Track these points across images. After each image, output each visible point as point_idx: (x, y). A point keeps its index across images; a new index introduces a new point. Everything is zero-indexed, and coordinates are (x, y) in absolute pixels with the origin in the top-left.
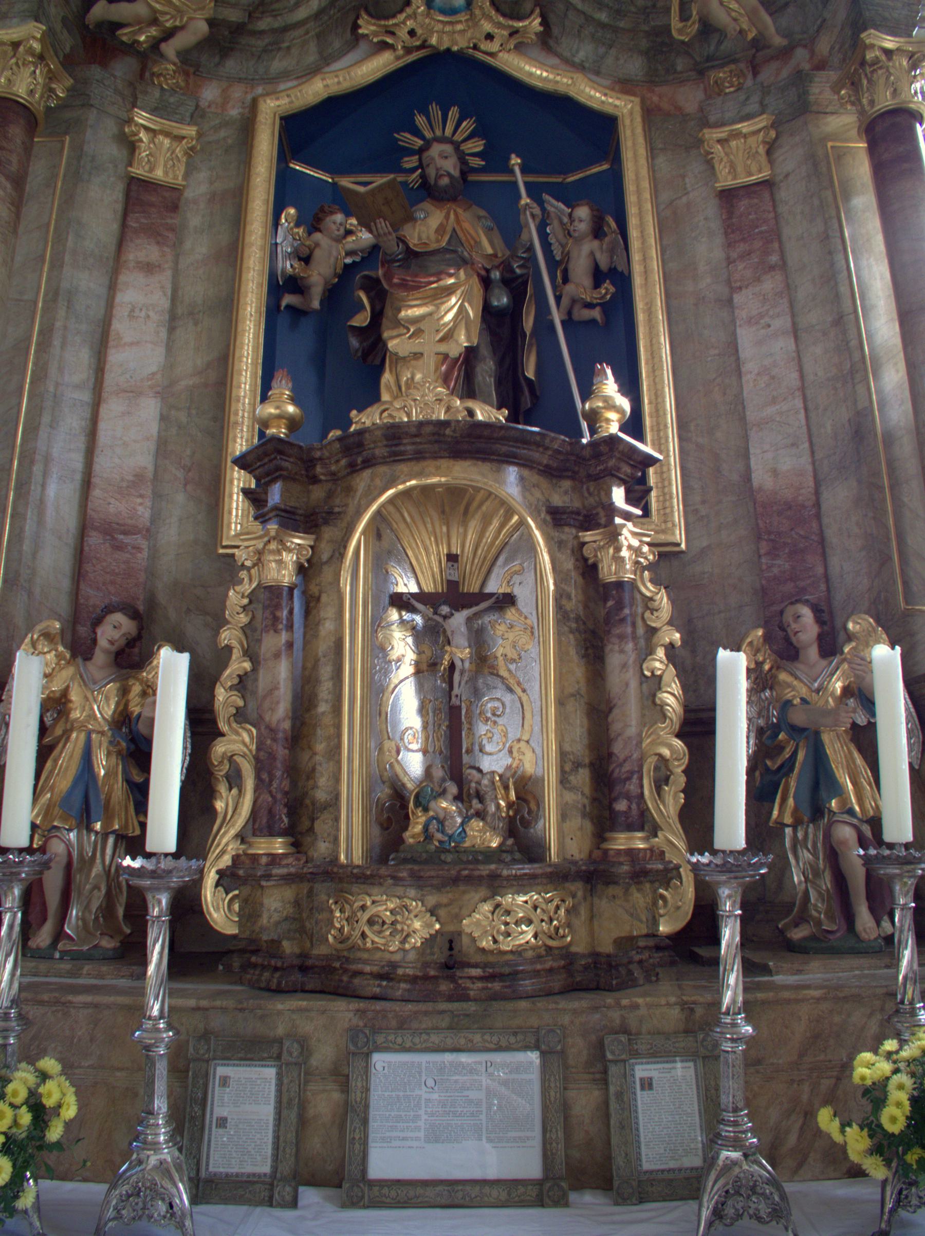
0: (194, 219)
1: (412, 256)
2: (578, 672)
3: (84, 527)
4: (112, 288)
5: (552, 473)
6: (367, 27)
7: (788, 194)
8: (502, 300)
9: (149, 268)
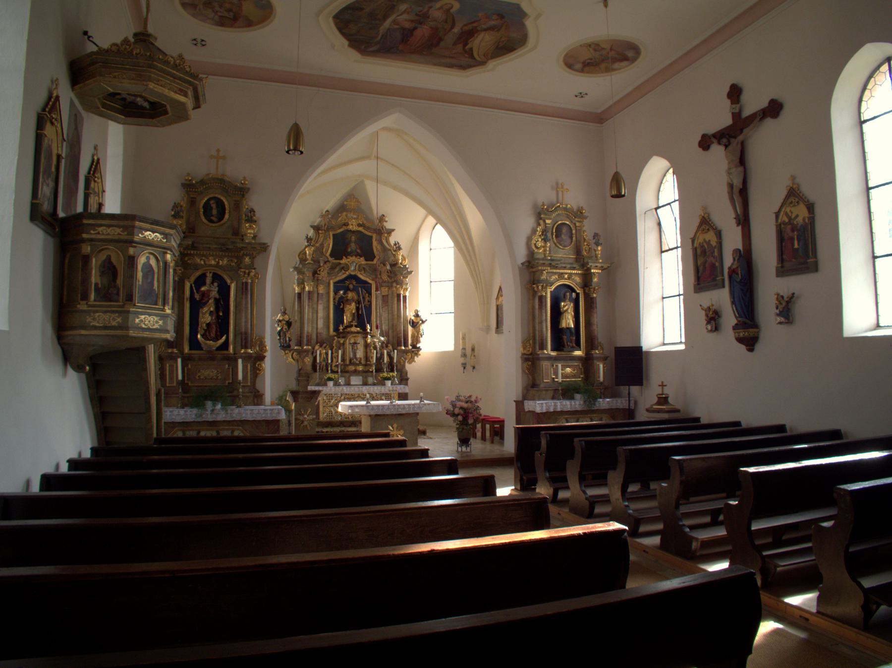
0: (324, 296)
1: (347, 300)
2: (365, 350)
3: (317, 333)
5: (363, 334)
6: (343, 271)
7: (390, 297)
8: (358, 305)
9: (321, 304)
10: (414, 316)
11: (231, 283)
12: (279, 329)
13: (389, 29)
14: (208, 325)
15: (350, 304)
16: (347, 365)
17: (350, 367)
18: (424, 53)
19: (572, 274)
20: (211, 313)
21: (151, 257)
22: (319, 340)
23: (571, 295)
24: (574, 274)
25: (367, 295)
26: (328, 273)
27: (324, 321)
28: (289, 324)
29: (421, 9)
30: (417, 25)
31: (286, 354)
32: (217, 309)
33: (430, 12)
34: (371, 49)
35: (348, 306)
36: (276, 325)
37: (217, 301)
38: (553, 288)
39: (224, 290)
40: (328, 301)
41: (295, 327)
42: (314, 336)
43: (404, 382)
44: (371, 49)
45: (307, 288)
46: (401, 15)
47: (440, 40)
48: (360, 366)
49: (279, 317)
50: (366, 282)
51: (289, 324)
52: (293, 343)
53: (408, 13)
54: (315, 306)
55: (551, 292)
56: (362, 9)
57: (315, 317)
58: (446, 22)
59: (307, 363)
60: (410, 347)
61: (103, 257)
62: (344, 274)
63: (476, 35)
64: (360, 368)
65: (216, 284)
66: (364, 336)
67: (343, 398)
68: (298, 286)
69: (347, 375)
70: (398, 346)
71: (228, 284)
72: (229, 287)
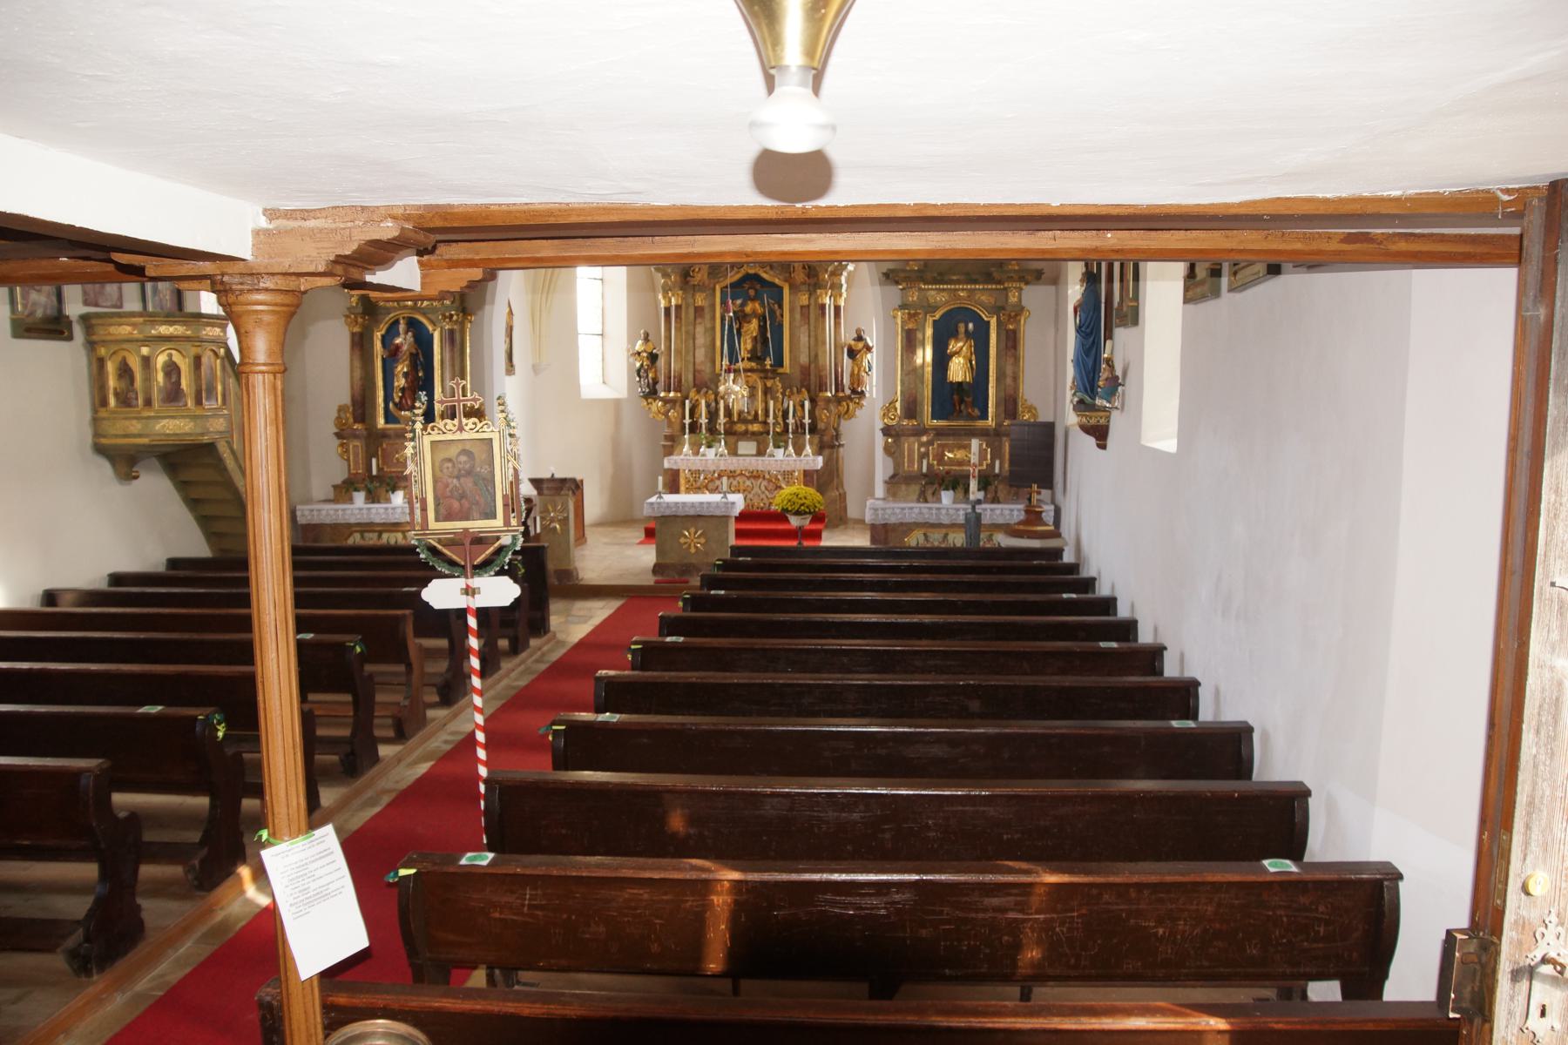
0: (706, 310)
2: (764, 398)
3: (695, 371)
4: (695, 328)
7: (812, 307)
9: (700, 323)
10: (854, 340)
11: (434, 330)
12: (638, 365)
14: (403, 390)
15: (749, 322)
16: (735, 423)
17: (739, 425)
19: (975, 289)
20: (406, 375)
21: (174, 352)
22: (697, 382)
23: (967, 327)
24: (979, 289)
25: (776, 306)
26: (709, 274)
27: (706, 351)
28: (653, 358)
31: (648, 404)
32: (414, 366)
35: (746, 325)
36: (631, 360)
37: (413, 358)
38: (937, 316)
39: (423, 343)
40: (713, 318)
41: (661, 362)
42: (691, 377)
43: (827, 452)
45: (673, 302)
48: (755, 425)
49: (639, 346)
50: (773, 285)
51: (653, 358)
52: (660, 387)
54: (691, 328)
55: (934, 321)
57: (691, 345)
59: (673, 420)
60: (848, 392)
61: (118, 358)
62: (738, 272)
64: (756, 427)
65: (410, 334)
66: (762, 375)
67: (716, 475)
68: (664, 297)
69: (732, 439)
70: (821, 390)
71: (431, 332)
72: (432, 335)
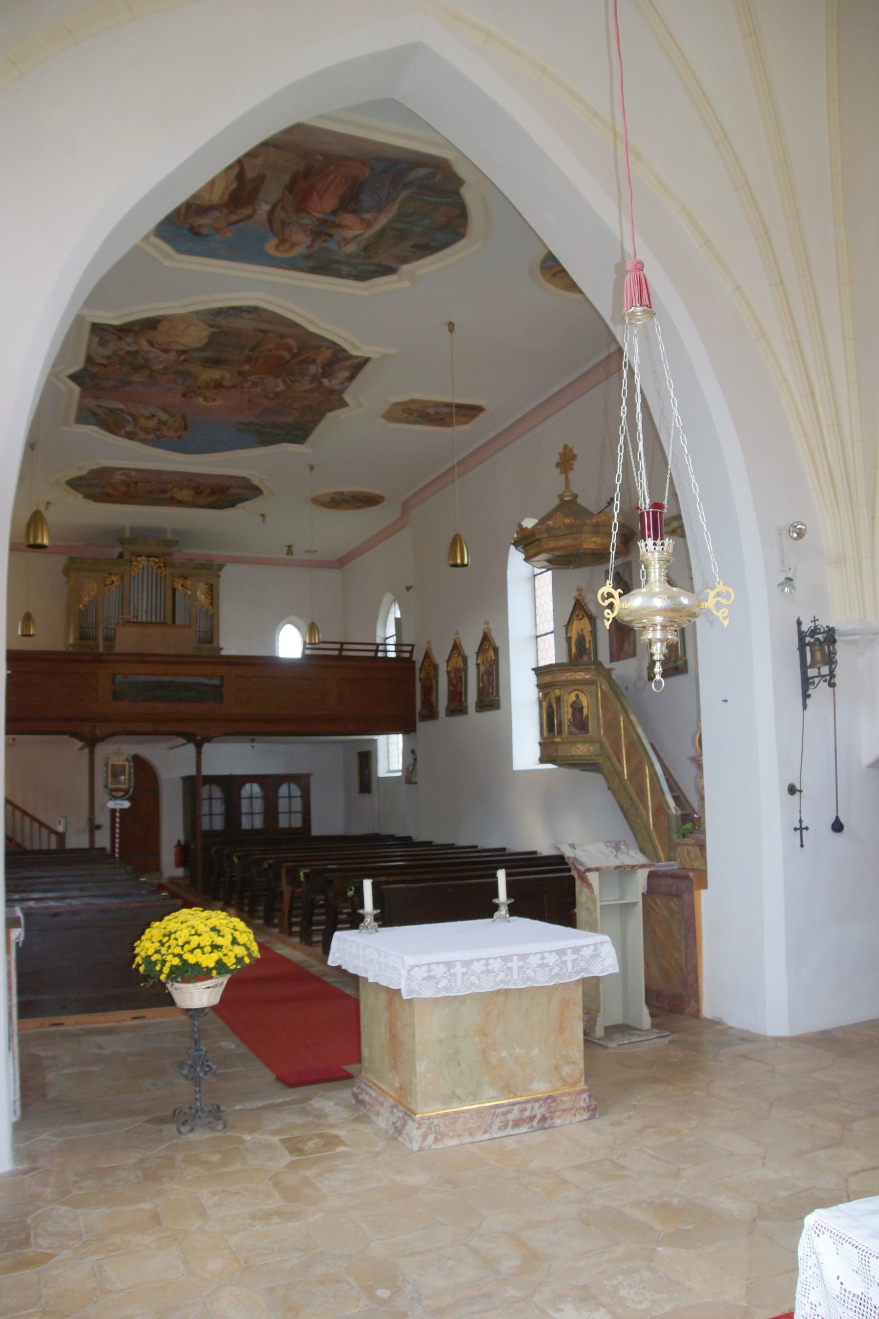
13: (380, 211)
18: (320, 158)
29: (325, 245)
30: (332, 218)
33: (311, 239)
34: (422, 172)
44: (422, 172)
46: (356, 237)
47: (291, 188)
53: (345, 239)
56: (414, 246)
58: (283, 223)
63: (227, 197)
